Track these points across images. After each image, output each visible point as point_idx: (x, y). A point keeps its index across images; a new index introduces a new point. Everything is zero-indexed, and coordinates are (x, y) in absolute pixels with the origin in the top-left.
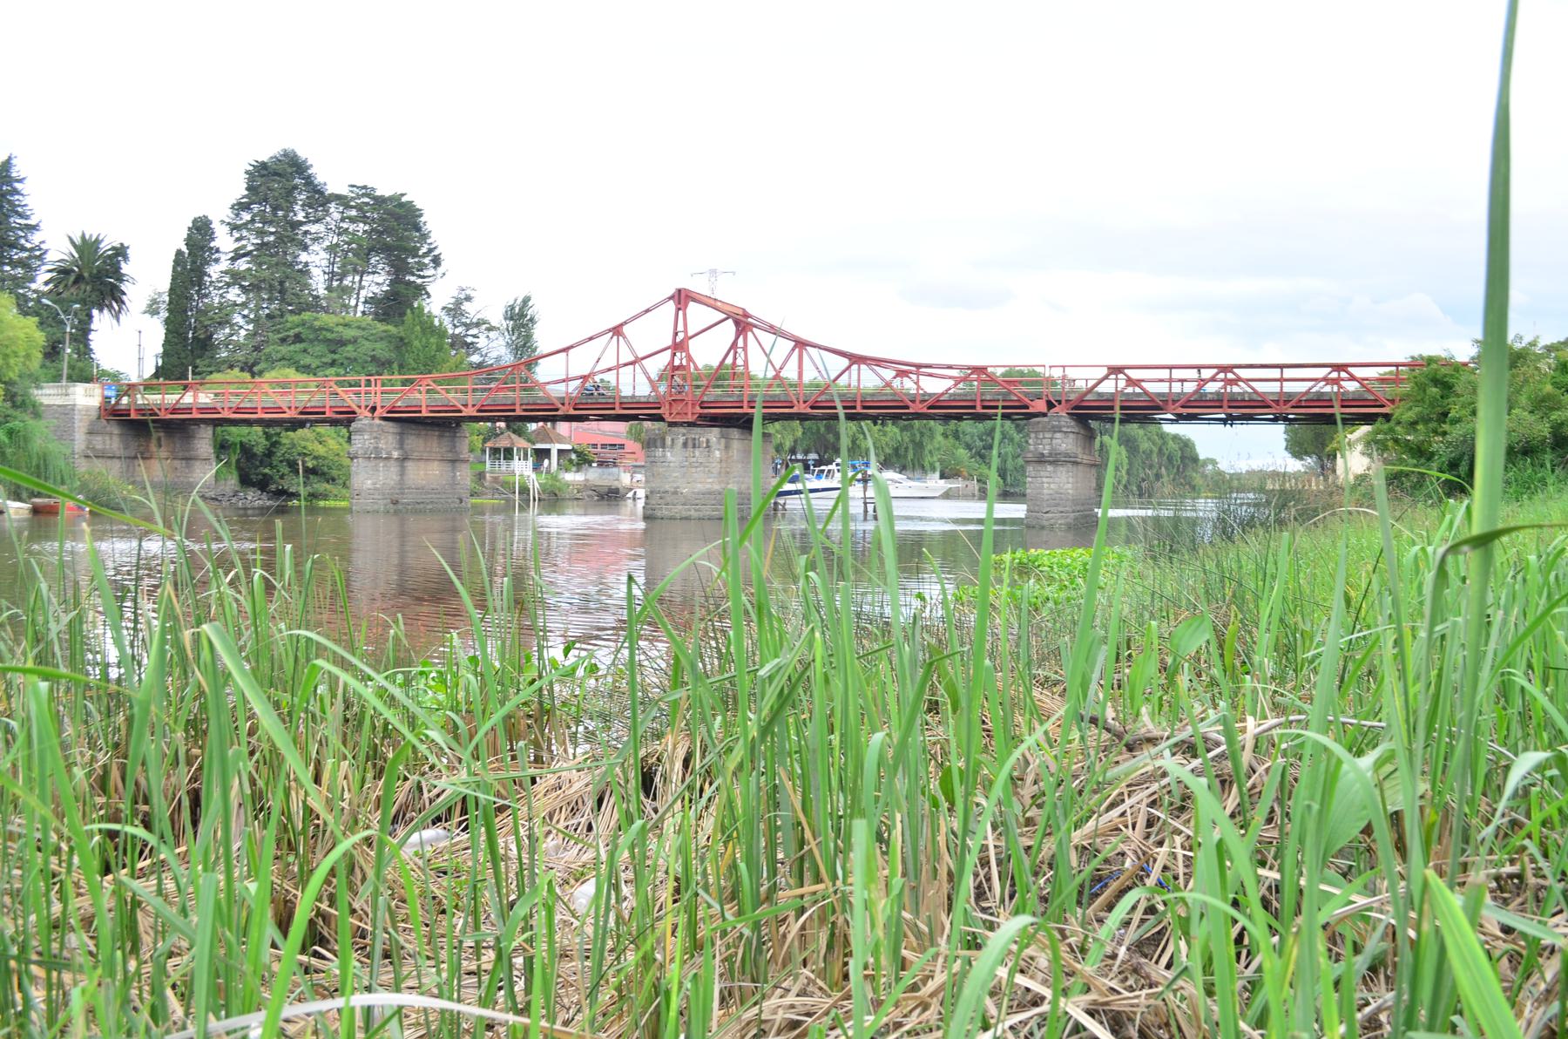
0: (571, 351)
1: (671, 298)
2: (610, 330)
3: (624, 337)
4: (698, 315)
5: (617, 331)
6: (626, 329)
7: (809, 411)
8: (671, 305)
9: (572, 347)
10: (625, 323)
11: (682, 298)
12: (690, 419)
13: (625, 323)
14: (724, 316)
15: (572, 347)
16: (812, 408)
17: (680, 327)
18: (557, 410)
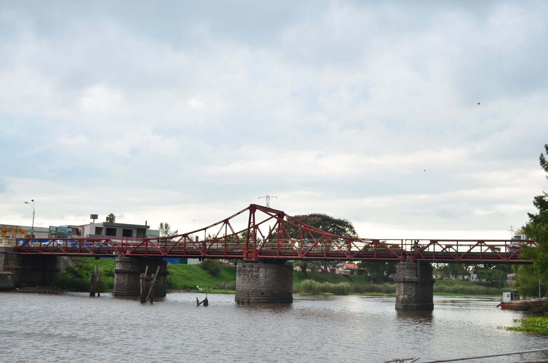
0: (207, 230)
1: (248, 208)
2: (223, 221)
3: (229, 224)
4: (260, 215)
5: (226, 221)
6: (230, 221)
7: (305, 257)
8: (248, 212)
9: (207, 228)
10: (230, 218)
11: (253, 208)
12: (254, 259)
13: (230, 218)
14: (271, 216)
15: (207, 228)
16: (306, 256)
17: (252, 221)
18: (201, 254)
